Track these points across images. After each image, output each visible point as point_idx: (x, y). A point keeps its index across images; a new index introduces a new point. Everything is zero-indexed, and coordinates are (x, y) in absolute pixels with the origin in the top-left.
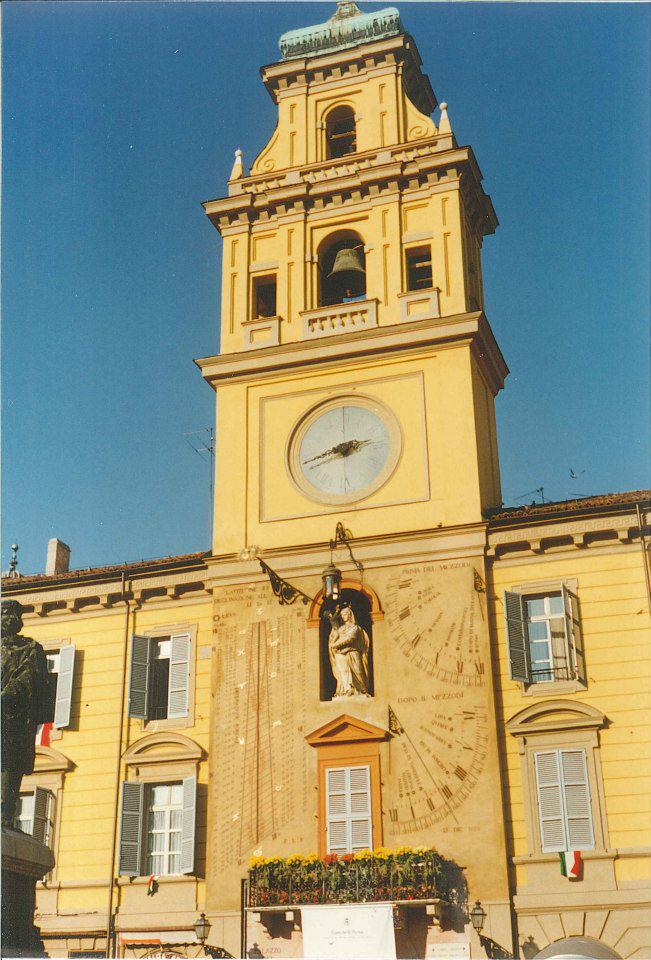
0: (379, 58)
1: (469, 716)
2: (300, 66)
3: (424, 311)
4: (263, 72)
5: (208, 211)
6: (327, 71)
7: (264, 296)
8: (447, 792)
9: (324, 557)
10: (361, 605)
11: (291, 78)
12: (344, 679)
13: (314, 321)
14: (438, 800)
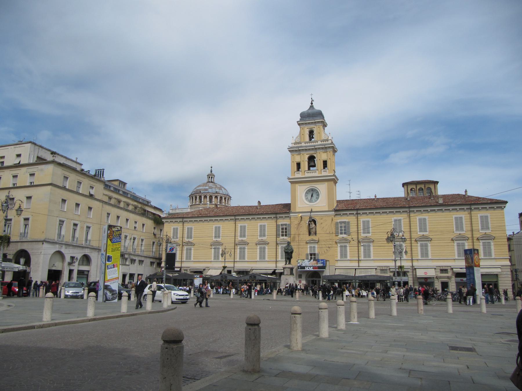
6: (309, 123)
9: (309, 214)
10: (315, 222)
12: (312, 233)
14: (326, 251)
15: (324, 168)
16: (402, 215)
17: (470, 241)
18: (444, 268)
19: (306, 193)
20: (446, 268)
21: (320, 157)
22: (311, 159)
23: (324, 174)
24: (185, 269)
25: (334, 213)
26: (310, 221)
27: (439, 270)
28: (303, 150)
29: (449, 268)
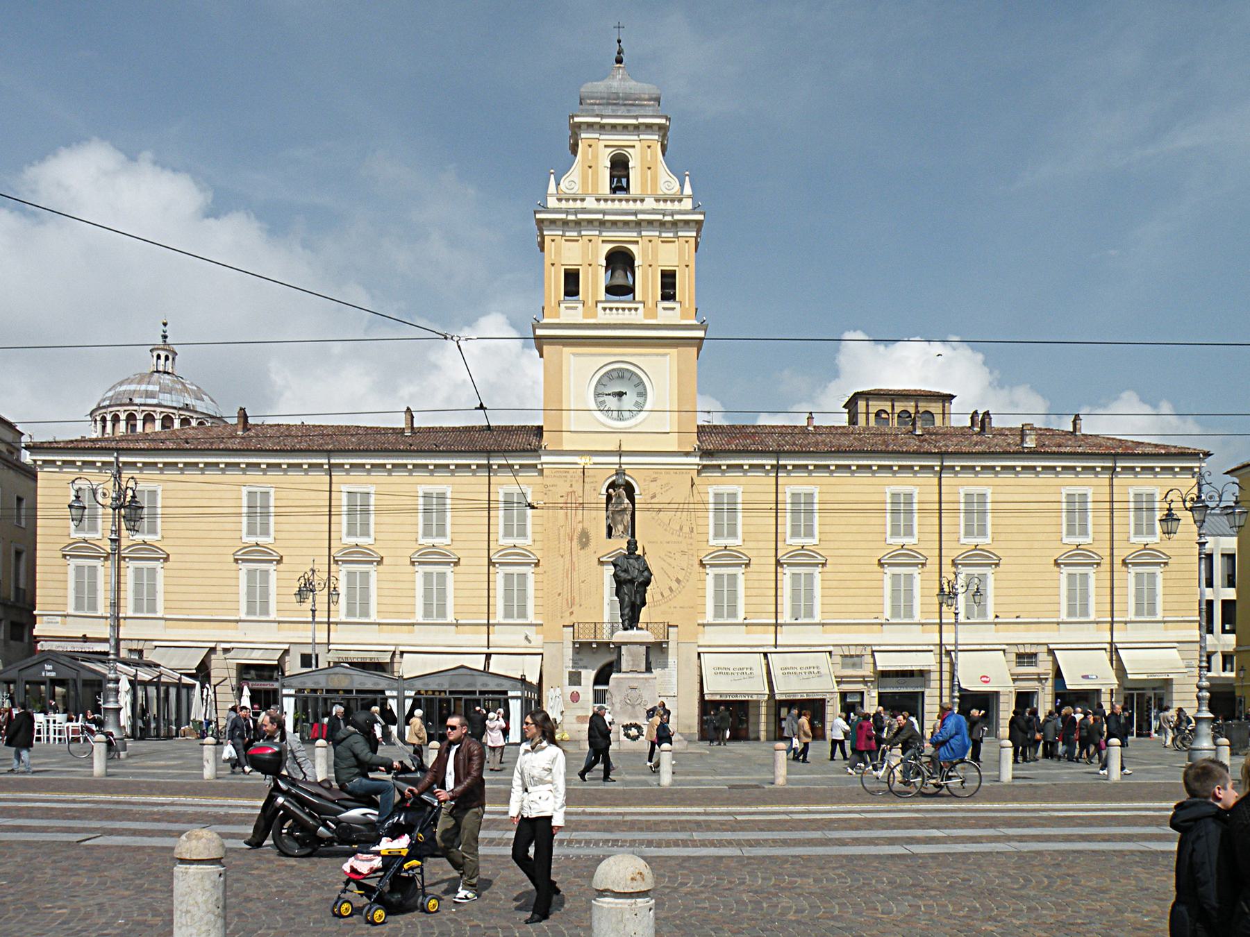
0: (649, 127)
1: (684, 553)
2: (598, 120)
3: (674, 318)
4: (573, 117)
5: (538, 216)
6: (614, 126)
7: (572, 282)
8: (671, 589)
10: (630, 490)
11: (590, 126)
13: (605, 309)
15: (665, 297)
16: (916, 480)
17: (1106, 567)
18: (1028, 650)
19: (599, 382)
20: (1033, 650)
21: (654, 256)
22: (620, 260)
23: (664, 317)
24: (134, 646)
25: (697, 460)
26: (613, 485)
27: (1013, 657)
28: (590, 222)
29: (1045, 648)
